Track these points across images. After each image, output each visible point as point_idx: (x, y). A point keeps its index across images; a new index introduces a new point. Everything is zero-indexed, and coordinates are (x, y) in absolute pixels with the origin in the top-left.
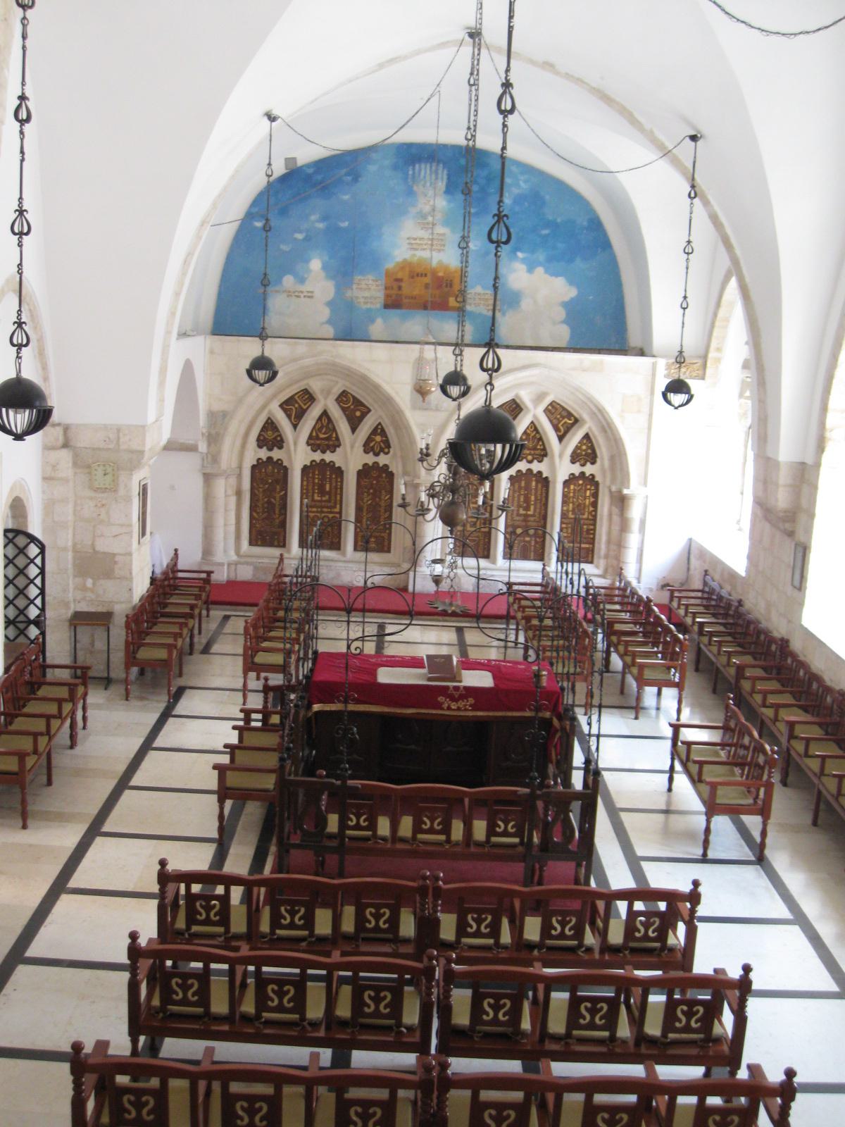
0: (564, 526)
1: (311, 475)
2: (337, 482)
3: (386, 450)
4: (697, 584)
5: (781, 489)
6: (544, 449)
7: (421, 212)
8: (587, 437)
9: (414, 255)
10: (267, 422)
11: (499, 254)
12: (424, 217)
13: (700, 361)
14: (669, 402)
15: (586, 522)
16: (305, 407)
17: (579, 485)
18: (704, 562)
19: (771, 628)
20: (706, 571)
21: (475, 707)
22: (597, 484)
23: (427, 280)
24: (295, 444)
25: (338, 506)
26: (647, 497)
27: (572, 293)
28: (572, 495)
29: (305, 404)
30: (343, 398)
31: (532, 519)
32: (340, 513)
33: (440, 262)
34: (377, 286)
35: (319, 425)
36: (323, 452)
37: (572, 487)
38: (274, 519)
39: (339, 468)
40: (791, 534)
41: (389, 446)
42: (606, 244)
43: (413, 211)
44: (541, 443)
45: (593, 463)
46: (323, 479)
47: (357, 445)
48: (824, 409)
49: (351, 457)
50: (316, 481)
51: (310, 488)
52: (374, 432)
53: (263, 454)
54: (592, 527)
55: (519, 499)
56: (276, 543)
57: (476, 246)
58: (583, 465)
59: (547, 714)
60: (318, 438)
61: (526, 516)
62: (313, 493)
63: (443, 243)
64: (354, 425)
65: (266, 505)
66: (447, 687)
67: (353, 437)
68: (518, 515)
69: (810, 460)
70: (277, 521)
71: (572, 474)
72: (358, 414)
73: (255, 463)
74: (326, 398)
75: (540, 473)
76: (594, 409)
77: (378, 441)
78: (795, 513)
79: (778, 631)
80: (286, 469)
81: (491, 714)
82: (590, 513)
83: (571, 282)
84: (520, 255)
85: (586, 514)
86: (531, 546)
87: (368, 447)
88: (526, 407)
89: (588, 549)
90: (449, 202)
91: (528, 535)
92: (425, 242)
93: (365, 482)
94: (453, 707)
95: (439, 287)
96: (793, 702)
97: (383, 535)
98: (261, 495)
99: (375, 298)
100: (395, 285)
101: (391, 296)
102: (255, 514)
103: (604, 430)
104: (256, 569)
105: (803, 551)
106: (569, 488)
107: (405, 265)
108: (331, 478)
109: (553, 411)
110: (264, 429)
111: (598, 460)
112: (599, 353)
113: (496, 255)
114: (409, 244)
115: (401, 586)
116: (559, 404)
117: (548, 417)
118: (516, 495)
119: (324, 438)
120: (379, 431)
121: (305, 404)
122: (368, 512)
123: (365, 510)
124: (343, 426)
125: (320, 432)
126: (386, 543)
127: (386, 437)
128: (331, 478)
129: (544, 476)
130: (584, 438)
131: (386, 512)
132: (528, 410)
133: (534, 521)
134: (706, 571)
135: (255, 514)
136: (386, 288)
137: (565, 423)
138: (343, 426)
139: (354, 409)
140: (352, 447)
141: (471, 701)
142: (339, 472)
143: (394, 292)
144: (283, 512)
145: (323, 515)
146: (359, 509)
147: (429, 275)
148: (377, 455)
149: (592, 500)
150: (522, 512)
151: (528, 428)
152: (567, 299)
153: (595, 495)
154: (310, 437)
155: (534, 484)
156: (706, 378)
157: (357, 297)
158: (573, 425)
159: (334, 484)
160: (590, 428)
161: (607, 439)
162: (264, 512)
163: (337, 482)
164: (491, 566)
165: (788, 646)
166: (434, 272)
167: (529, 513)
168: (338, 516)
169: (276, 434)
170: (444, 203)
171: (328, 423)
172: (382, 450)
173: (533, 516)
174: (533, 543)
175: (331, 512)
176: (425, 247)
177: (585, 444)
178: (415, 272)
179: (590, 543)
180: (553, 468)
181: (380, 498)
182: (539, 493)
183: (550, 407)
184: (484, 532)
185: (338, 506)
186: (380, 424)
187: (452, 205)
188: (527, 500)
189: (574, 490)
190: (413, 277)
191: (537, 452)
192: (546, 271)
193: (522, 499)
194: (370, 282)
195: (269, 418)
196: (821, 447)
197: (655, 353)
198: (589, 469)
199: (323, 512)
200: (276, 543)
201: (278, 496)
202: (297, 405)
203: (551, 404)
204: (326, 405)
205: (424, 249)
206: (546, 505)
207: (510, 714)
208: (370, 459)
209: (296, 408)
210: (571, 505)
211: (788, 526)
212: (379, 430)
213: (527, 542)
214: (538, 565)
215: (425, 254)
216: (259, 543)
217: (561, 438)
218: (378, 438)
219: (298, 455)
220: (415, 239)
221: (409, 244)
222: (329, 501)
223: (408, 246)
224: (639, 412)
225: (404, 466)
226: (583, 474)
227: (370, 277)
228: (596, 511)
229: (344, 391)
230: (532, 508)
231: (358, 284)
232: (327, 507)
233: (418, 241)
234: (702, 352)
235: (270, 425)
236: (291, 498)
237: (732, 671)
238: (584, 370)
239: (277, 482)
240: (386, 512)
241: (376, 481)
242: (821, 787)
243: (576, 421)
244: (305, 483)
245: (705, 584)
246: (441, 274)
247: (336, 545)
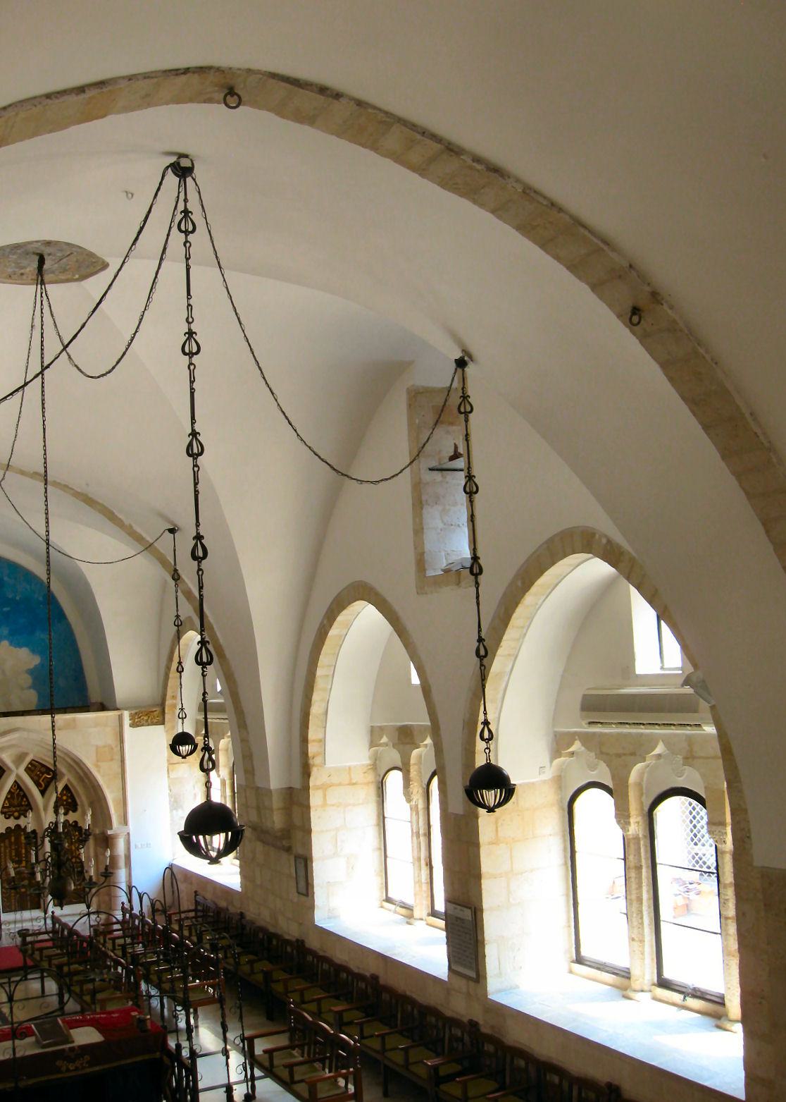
4: (187, 904)
5: (275, 813)
8: (66, 788)
11: (205, 673)
13: (158, 709)
14: (178, 754)
18: (191, 883)
19: (279, 932)
20: (196, 892)
21: (91, 1064)
26: (128, 834)
27: (35, 660)
40: (288, 850)
42: (61, 615)
44: (25, 799)
45: (75, 810)
48: (304, 740)
59: (158, 1055)
66: (63, 1050)
69: (297, 784)
76: (72, 763)
78: (289, 831)
79: (289, 934)
81: (106, 1066)
83: (33, 651)
88: (9, 769)
94: (71, 1068)
96: (327, 994)
103: (81, 779)
105: (304, 862)
109: (33, 768)
111: (79, 808)
112: (65, 713)
113: (202, 674)
116: (37, 762)
117: (28, 774)
118: (7, 851)
134: (196, 892)
141: (87, 1057)
151: (11, 787)
152: (32, 667)
156: (166, 723)
160: (69, 780)
161: (85, 787)
165: (304, 946)
177: (65, 795)
191: (23, 808)
192: (11, 644)
193: (13, 854)
196: (306, 771)
197: (118, 706)
203: (30, 763)
207: (123, 1062)
211: (285, 843)
214: (37, 913)
217: (43, 793)
224: (112, 760)
234: (159, 701)
237: (260, 977)
242: (386, 1062)
245: (197, 903)
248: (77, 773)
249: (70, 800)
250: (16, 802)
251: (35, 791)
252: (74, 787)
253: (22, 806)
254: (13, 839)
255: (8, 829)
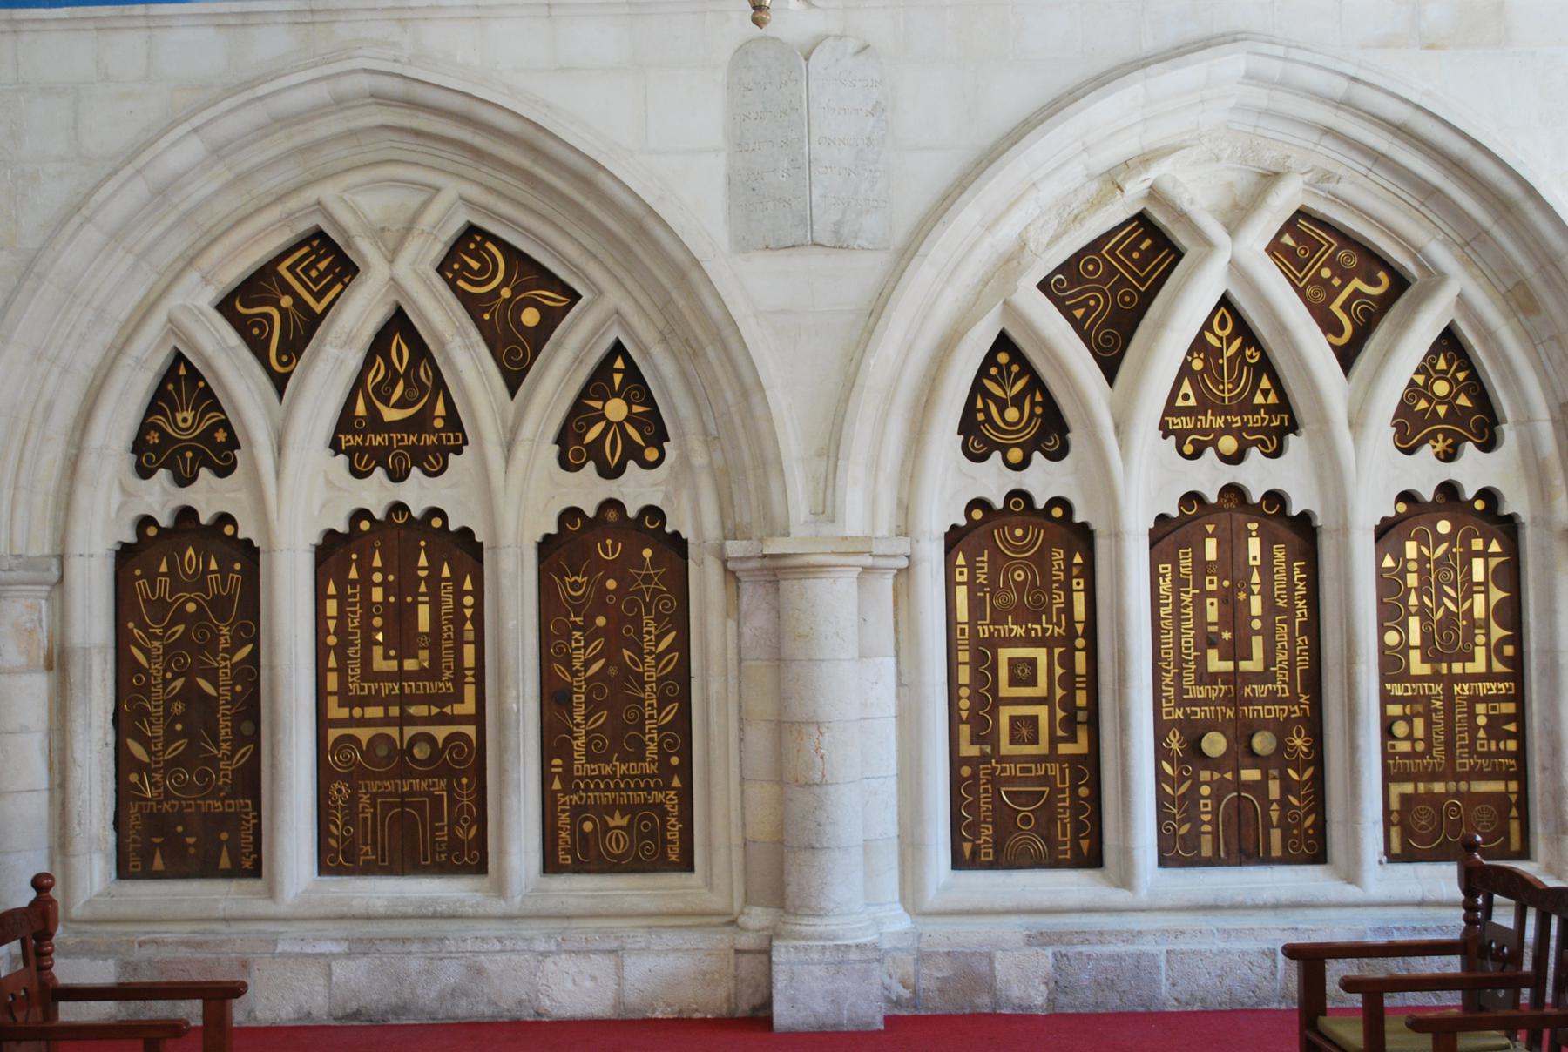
0: (1394, 710)
1: (353, 574)
2: (459, 594)
3: (651, 454)
6: (1284, 404)
8: (1449, 341)
10: (170, 375)
15: (1483, 688)
16: (318, 308)
17: (1440, 539)
22: (1509, 528)
24: (280, 449)
25: (470, 692)
28: (1412, 580)
29: (318, 297)
30: (467, 254)
31: (1261, 690)
32: (479, 719)
35: (379, 371)
36: (398, 476)
37: (1411, 549)
38: (213, 761)
39: (466, 533)
41: (658, 436)
44: (1265, 383)
45: (1489, 444)
46: (403, 585)
47: (527, 431)
49: (511, 486)
50: (377, 595)
51: (354, 623)
52: (597, 384)
53: (159, 497)
54: (1508, 708)
55: (1200, 611)
56: (225, 862)
58: (1449, 456)
60: (375, 422)
61: (1235, 679)
62: (369, 643)
64: (515, 358)
65: (178, 708)
67: (512, 406)
68: (1205, 678)
70: (227, 768)
71: (1407, 497)
72: (530, 317)
73: (130, 537)
74: (392, 257)
75: (1276, 498)
77: (617, 416)
80: (250, 552)
82: (1494, 650)
85: (1480, 653)
86: (1266, 802)
87: (573, 445)
89: (1501, 799)
91: (1255, 759)
93: (576, 585)
97: (658, 796)
98: (156, 668)
102: (137, 749)
104: (124, 966)
106: (1399, 555)
108: (434, 579)
110: (161, 400)
111: (1509, 433)
115: (744, 1008)
118: (1187, 599)
119: (399, 417)
120: (618, 378)
121: (318, 297)
122: (592, 708)
123: (579, 699)
124: (468, 364)
125: (386, 402)
126: (674, 834)
127: (649, 400)
128: (434, 579)
129: (1295, 510)
130: (1435, 349)
131: (663, 701)
132: (1208, 244)
133: (1273, 698)
135: (137, 749)
137: (1357, 293)
138: (468, 364)
139: (511, 293)
140: (509, 448)
142: (466, 550)
144: (247, 728)
145: (410, 731)
146: (554, 697)
148: (611, 472)
149: (1497, 595)
150: (1215, 663)
153: (1511, 574)
154: (346, 421)
155: (1254, 546)
158: (1386, 302)
159: (448, 605)
160: (1462, 301)
162: (171, 736)
163: (459, 594)
164: (1119, 897)
167: (1245, 666)
168: (470, 730)
169: (212, 418)
171: (414, 364)
172: (633, 452)
173: (1265, 677)
174: (1274, 789)
175: (443, 720)
177: (1442, 375)
179: (1506, 777)
180: (1329, 469)
181: (639, 652)
182: (1280, 581)
183: (1288, 240)
184: (1073, 759)
185: (470, 692)
186: (618, 349)
188: (1234, 612)
189: (1422, 559)
191: (1255, 420)
193: (1212, 614)
195: (179, 357)
198: (1473, 470)
199: (413, 720)
200: (225, 862)
201: (224, 667)
202: (286, 301)
203: (1290, 226)
204: (394, 282)
206: (1313, 627)
208: (586, 490)
209: (284, 313)
210: (1414, 623)
212: (616, 372)
213: (1251, 786)
216: (158, 864)
217: (1347, 357)
218: (616, 409)
219: (296, 490)
222: (432, 673)
225: (725, 505)
226: (1449, 490)
228: (1517, 637)
229: (471, 230)
230: (1257, 643)
232: (427, 700)
235: (182, 383)
236: (272, 668)
238: (1431, 47)
239: (220, 606)
240: (663, 701)
241: (619, 577)
243: (1400, 283)
244: (332, 607)
247: (469, 855)
248: (1508, 268)
249: (1463, 401)
250: (1225, 391)
251: (1316, 348)
252: (1487, 334)
253: (1256, 410)
254: (1211, 550)
255: (1191, 498)
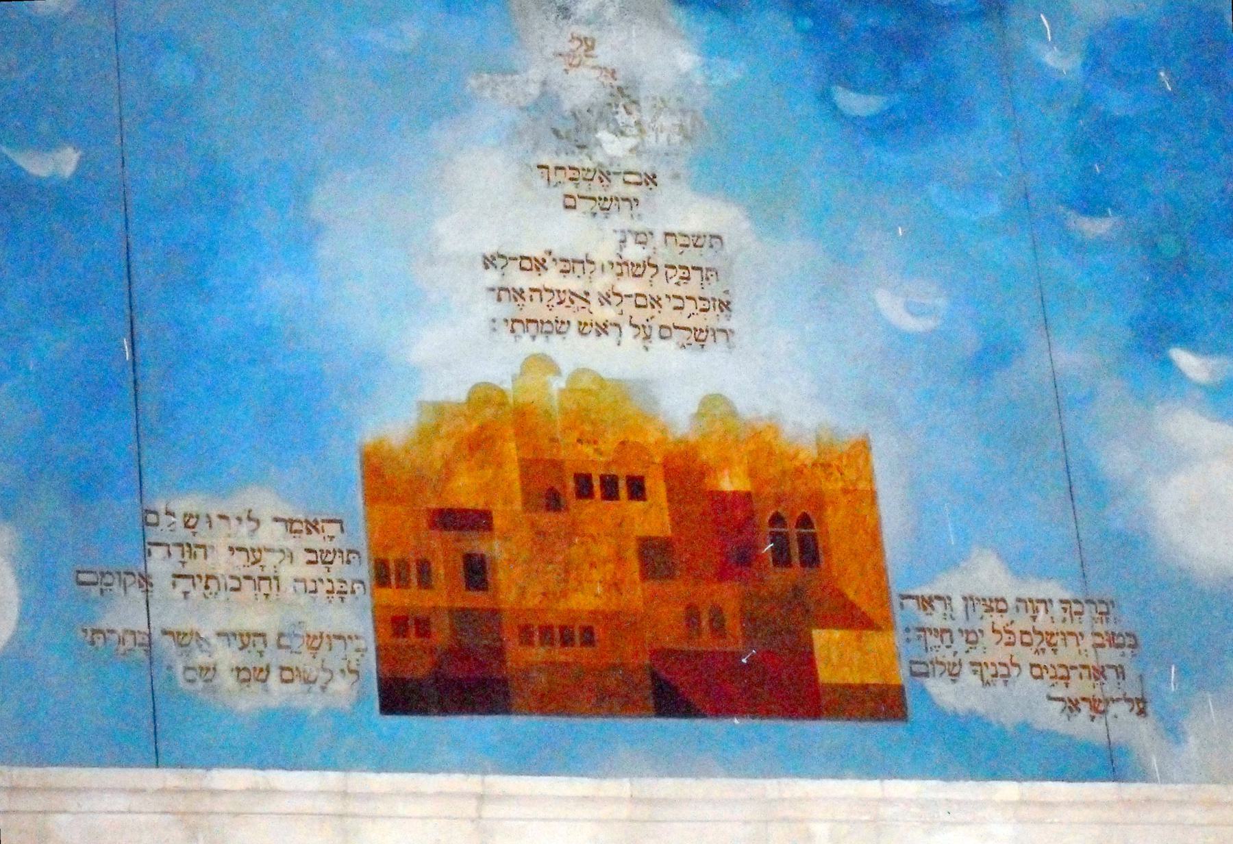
7: (547, 99)
9: (546, 364)
12: (575, 131)
23: (652, 517)
33: (713, 405)
34: (318, 557)
43: (498, 103)
57: (914, 310)
63: (714, 290)
84: (1184, 359)
90: (710, 50)
92: (601, 283)
95: (739, 563)
99: (315, 642)
100: (443, 551)
101: (423, 627)
107: (485, 425)
114: (500, 292)
136: (382, 576)
143: (441, 597)
147: (657, 488)
157: (179, 637)
166: (685, 473)
170: (686, 60)
176: (608, 313)
178: (573, 478)
187: (733, 71)
190: (553, 501)
194: (270, 534)
205: (602, 329)
215: (614, 358)
220: (539, 265)
221: (500, 292)
223: (489, 308)
227: (267, 504)
231: (189, 549)
233: (552, 278)
246: (731, 482)
